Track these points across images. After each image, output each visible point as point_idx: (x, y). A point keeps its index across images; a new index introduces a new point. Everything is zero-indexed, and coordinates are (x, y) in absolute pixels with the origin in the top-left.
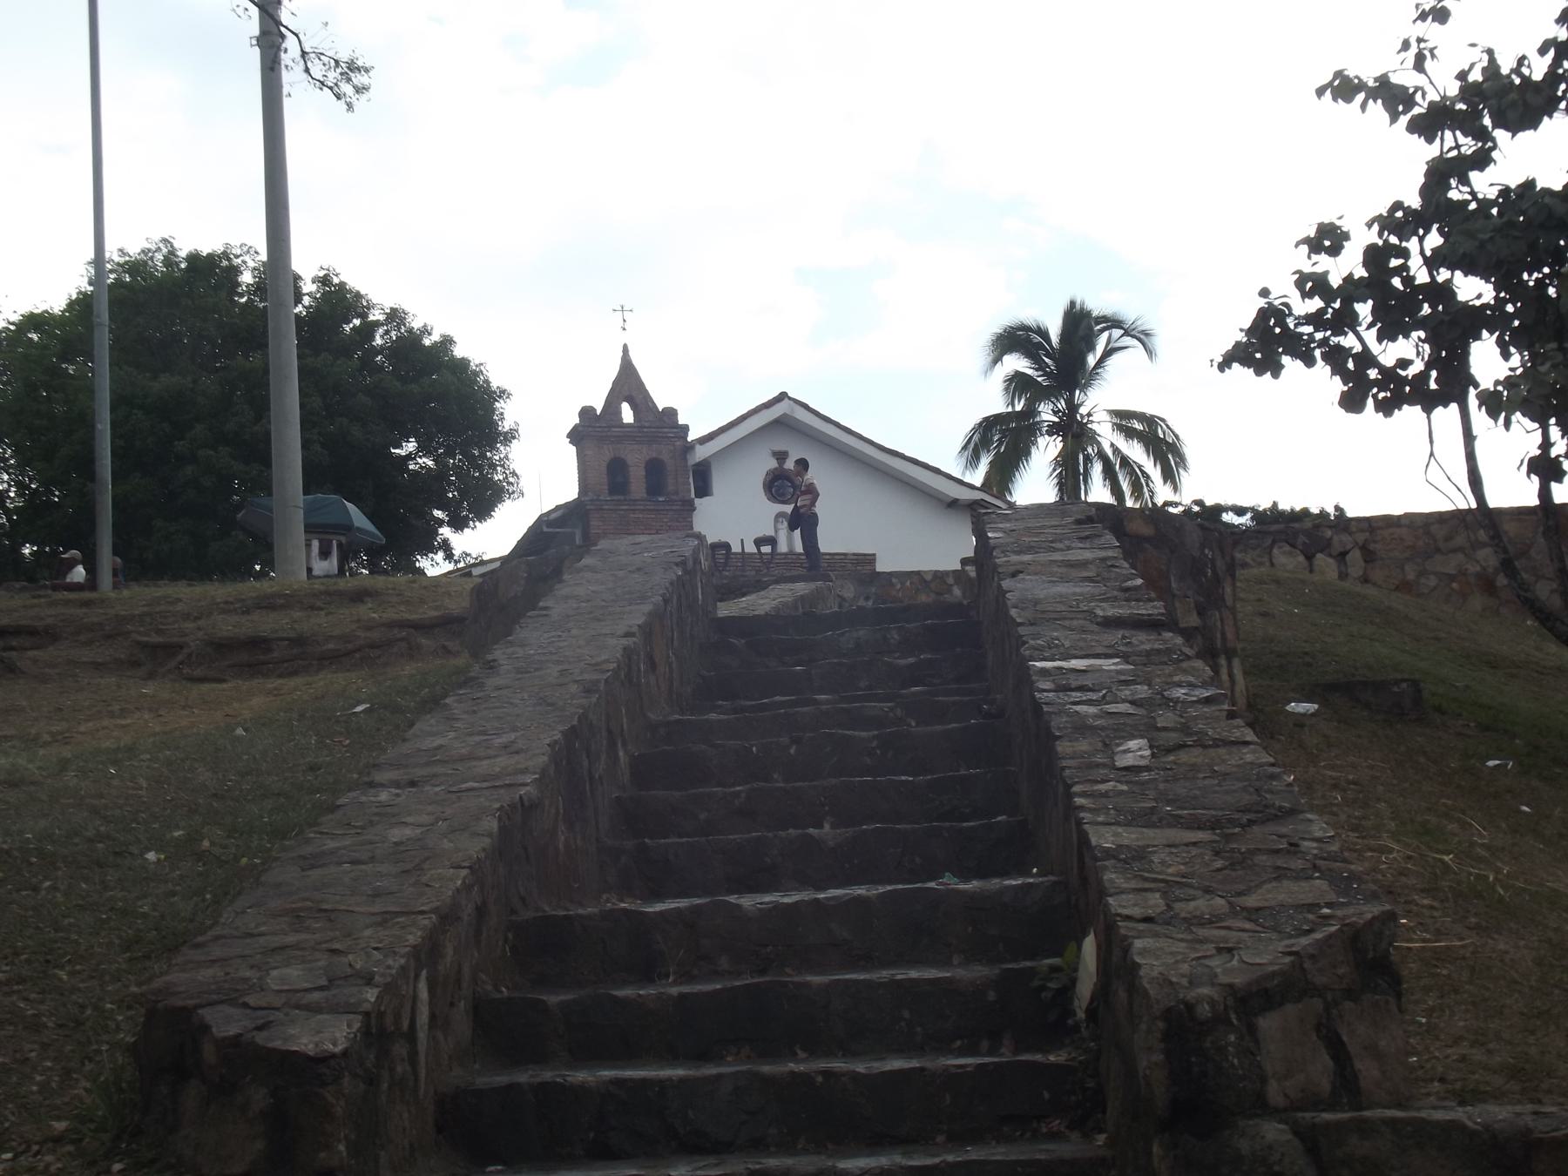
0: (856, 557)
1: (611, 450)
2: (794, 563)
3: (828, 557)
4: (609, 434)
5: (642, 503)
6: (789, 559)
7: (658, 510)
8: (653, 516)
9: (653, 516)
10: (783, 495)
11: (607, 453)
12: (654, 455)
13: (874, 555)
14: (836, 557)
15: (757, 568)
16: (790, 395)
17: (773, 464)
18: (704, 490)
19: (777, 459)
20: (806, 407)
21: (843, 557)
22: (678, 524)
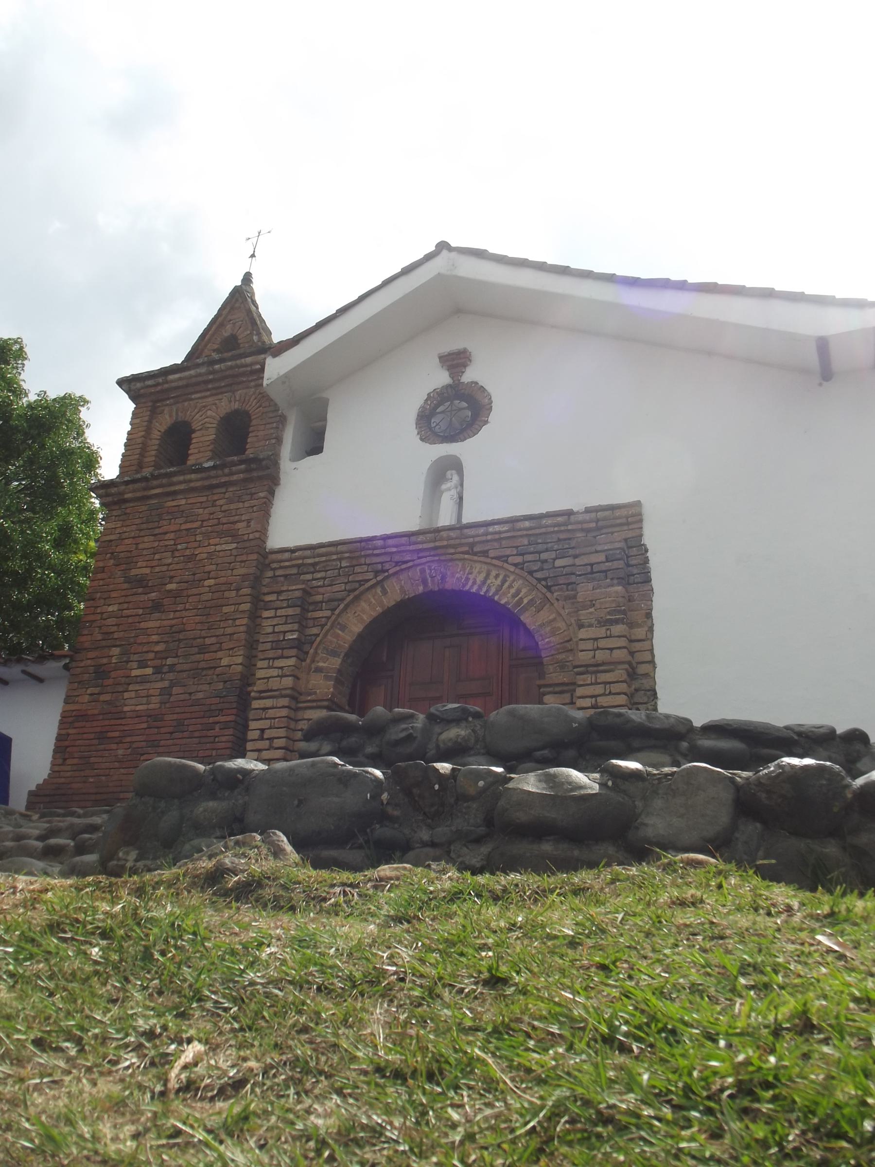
0: (593, 515)
1: (174, 414)
2: (454, 546)
3: (527, 524)
4: (166, 386)
5: (181, 478)
6: (442, 539)
7: (211, 487)
8: (204, 499)
9: (204, 499)
12: (236, 406)
13: (638, 504)
15: (379, 567)
16: (453, 244)
17: (443, 378)
20: (480, 254)
21: (560, 519)
22: (241, 505)
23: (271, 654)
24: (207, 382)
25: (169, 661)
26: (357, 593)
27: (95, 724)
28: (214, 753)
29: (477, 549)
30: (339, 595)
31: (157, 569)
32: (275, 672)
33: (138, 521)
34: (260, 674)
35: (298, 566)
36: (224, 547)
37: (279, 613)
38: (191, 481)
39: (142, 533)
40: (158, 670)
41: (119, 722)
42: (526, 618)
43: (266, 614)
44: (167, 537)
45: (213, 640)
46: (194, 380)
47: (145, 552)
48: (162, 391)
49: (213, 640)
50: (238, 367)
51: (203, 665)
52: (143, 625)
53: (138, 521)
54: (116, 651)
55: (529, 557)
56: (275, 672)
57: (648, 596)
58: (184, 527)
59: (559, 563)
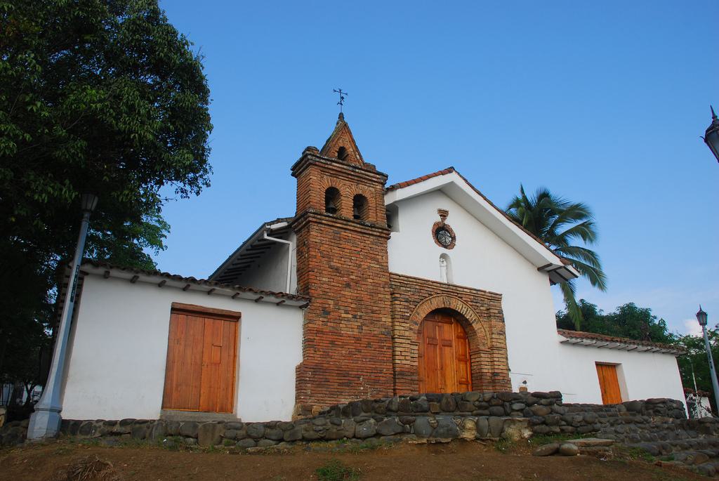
3: (474, 292)
5: (353, 224)
12: (361, 192)
13: (501, 295)
14: (479, 292)
17: (439, 219)
19: (441, 216)
21: (483, 293)
23: (401, 320)
24: (349, 174)
25: (359, 314)
26: (424, 301)
27: (328, 336)
28: (385, 359)
29: (459, 295)
30: (417, 300)
31: (345, 266)
32: (403, 328)
33: (330, 237)
34: (397, 328)
35: (400, 283)
36: (373, 265)
37: (402, 303)
38: (355, 227)
39: (333, 244)
40: (355, 317)
41: (340, 338)
43: (397, 302)
44: (346, 250)
45: (377, 308)
46: (344, 171)
47: (336, 255)
48: (328, 168)
49: (377, 308)
50: (366, 175)
51: (374, 319)
52: (342, 292)
53: (330, 237)
54: (331, 302)
55: (474, 304)
56: (403, 328)
58: (353, 248)
59: (482, 308)
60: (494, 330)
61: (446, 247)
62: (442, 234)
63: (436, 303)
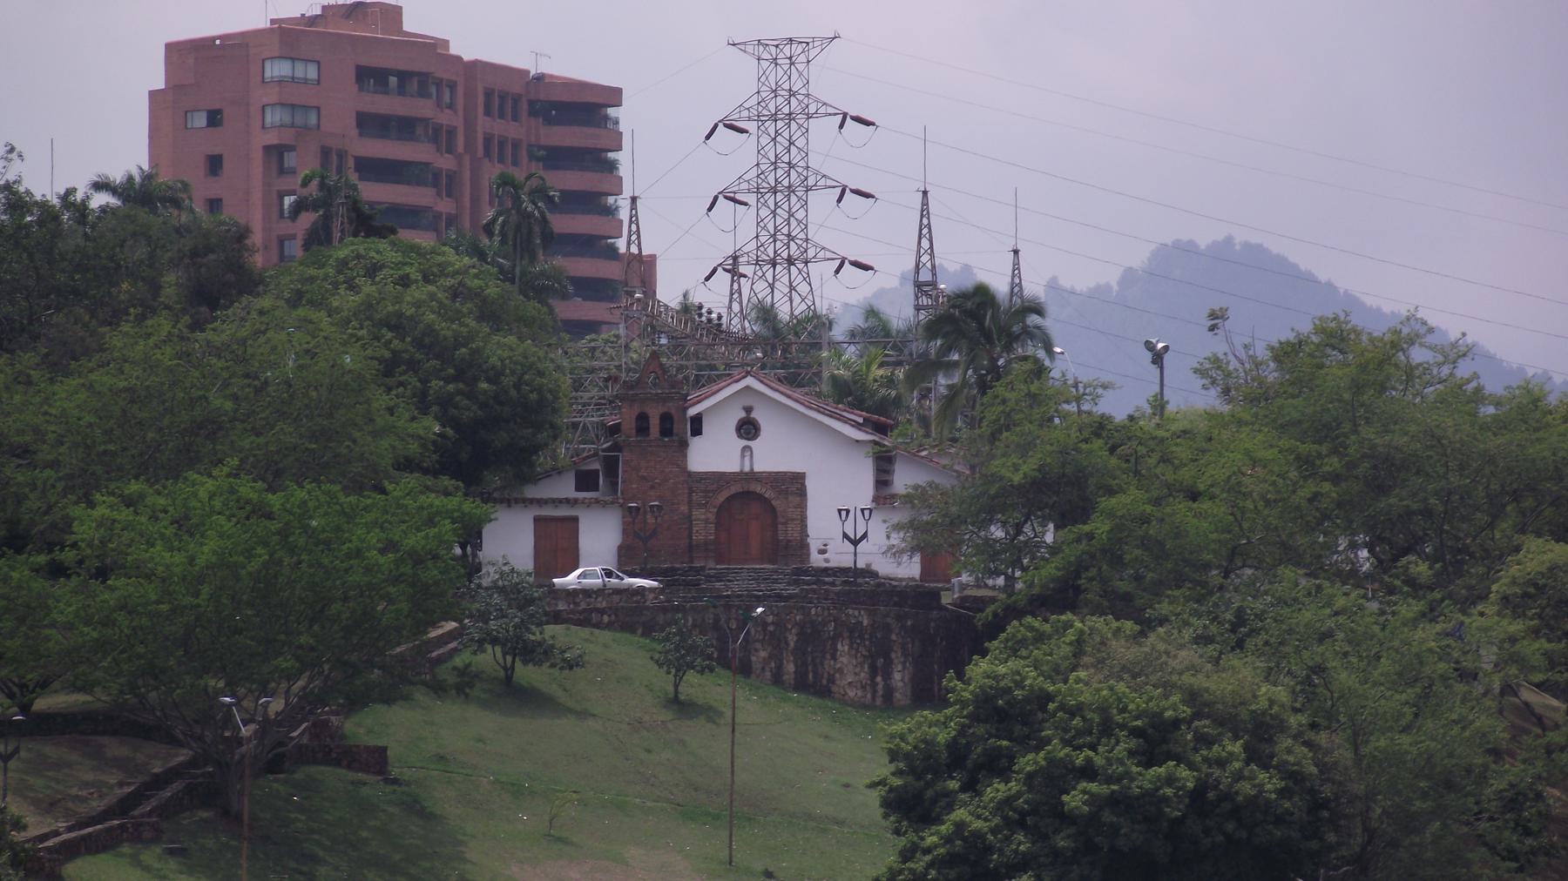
10: (748, 434)
11: (636, 411)
12: (666, 410)
17: (743, 414)
18: (697, 430)
42: (773, 502)
57: (806, 500)
60: (791, 505)
61: (749, 439)
62: (748, 428)
63: (735, 489)
